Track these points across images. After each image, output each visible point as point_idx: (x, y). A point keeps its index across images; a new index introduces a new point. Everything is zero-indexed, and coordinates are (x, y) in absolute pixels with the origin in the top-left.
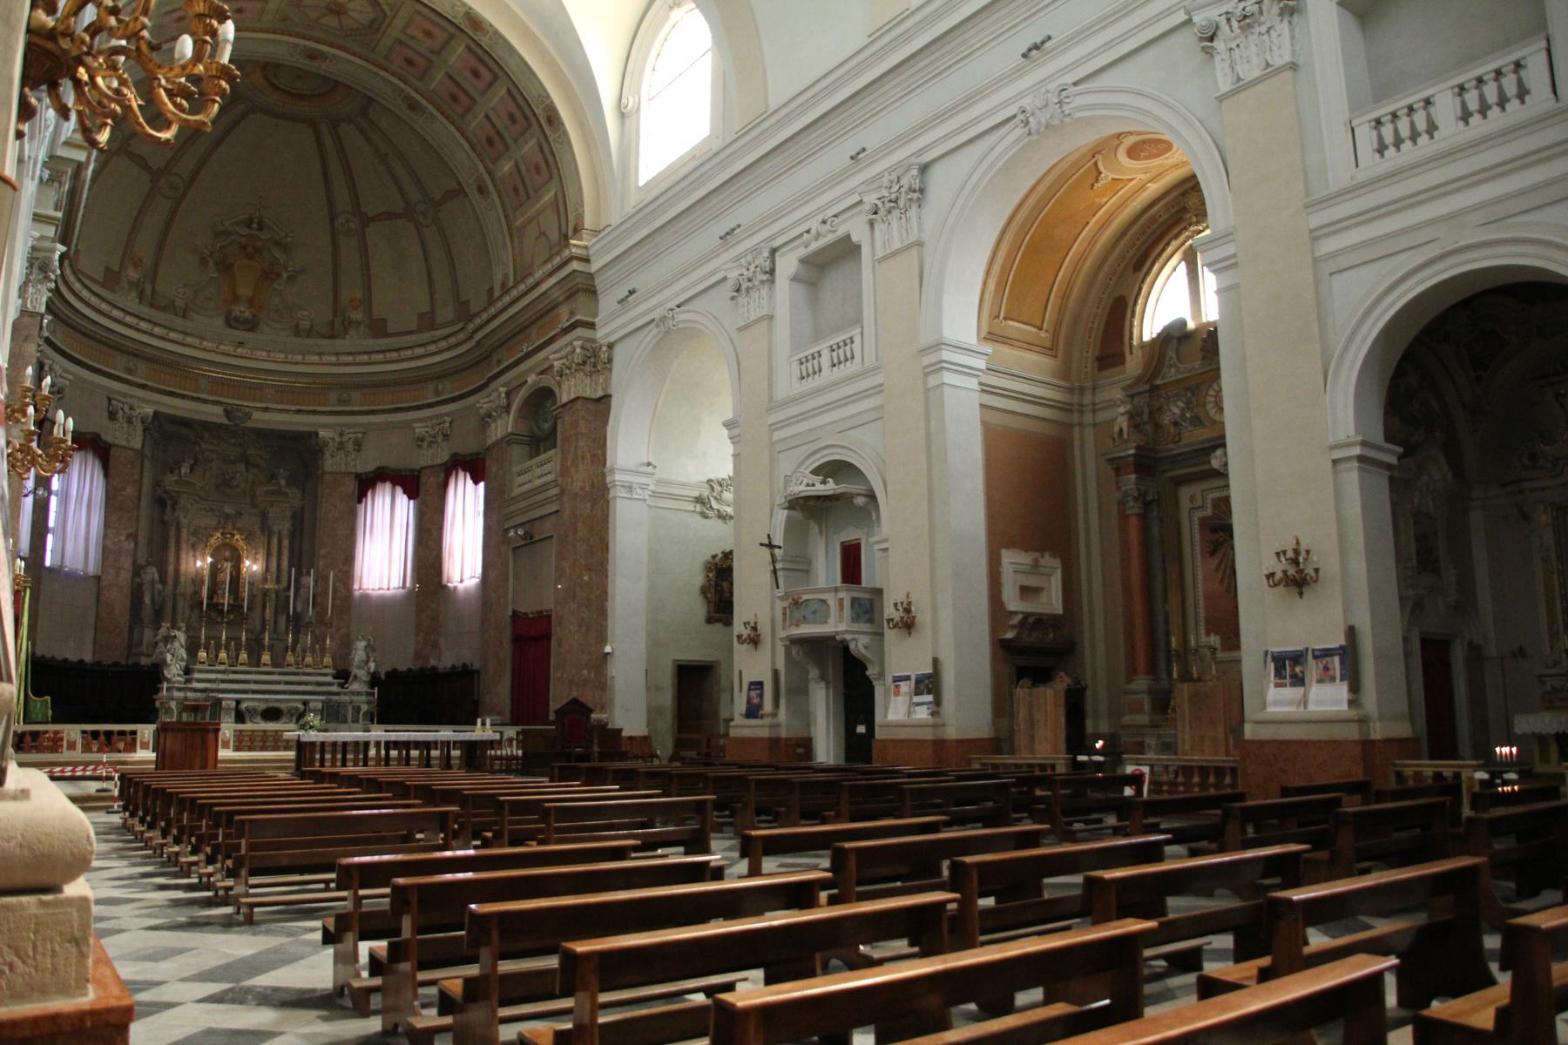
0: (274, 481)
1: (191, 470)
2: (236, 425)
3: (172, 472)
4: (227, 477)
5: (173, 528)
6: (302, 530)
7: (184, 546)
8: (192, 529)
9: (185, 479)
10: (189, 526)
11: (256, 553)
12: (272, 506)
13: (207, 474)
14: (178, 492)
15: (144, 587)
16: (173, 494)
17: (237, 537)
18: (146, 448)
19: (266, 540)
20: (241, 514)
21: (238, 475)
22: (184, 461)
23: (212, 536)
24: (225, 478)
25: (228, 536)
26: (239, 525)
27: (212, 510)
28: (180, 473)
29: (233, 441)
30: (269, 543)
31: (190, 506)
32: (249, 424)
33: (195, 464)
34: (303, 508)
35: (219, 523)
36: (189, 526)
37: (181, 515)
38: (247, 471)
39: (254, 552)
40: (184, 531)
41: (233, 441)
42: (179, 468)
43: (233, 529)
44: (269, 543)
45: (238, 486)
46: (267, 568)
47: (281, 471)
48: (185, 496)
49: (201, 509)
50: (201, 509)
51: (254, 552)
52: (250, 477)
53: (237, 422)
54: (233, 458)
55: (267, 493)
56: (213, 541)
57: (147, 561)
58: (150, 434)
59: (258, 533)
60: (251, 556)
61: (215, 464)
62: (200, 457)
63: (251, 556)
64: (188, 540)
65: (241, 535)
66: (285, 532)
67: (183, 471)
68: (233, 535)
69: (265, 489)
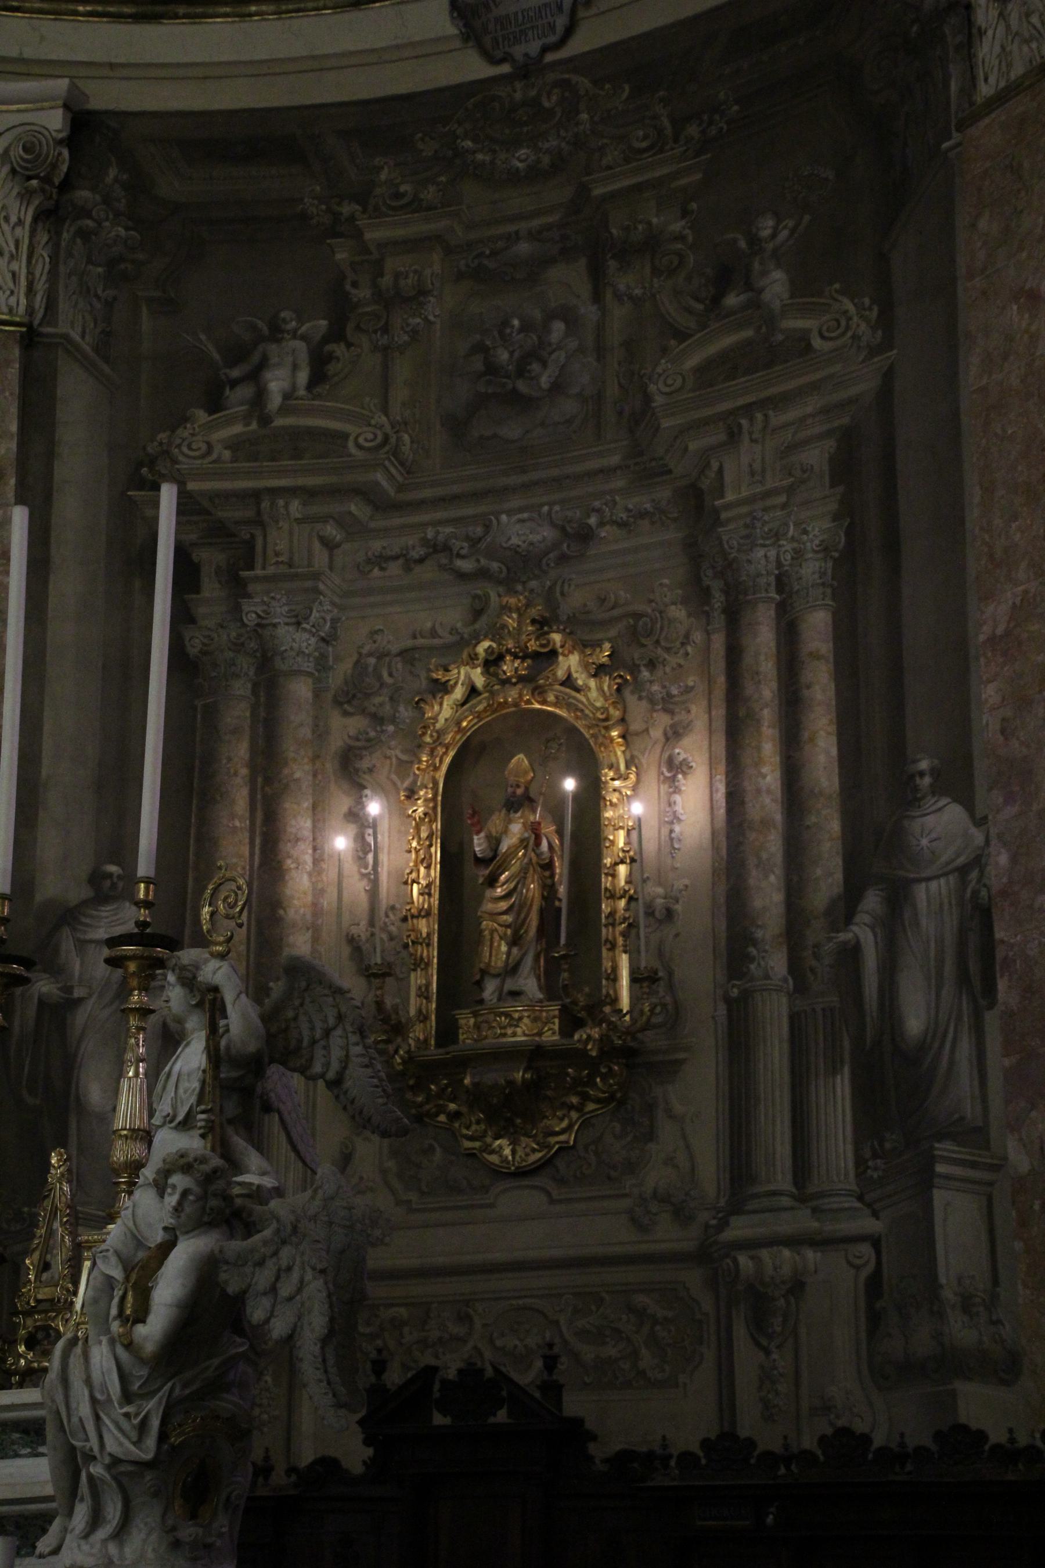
0: (732, 300)
1: (317, 377)
2: (526, 71)
3: (214, 404)
4: (504, 356)
5: (241, 688)
6: (892, 546)
7: (299, 770)
8: (342, 671)
9: (279, 422)
10: (322, 664)
11: (674, 734)
12: (734, 436)
13: (403, 370)
14: (256, 495)
15: (80, 1017)
16: (229, 514)
17: (571, 663)
18: (63, 306)
19: (719, 642)
20: (585, 536)
21: (558, 328)
22: (276, 333)
23: (443, 688)
24: (492, 369)
25: (508, 667)
26: (576, 599)
27: (437, 548)
28: (260, 396)
29: (521, 158)
30: (734, 654)
31: (320, 557)
32: (579, 45)
33: (336, 334)
34: (885, 394)
35: (477, 613)
36: (322, 664)
37: (280, 611)
38: (597, 297)
39: (657, 733)
40: (301, 690)
41: (521, 158)
42: (255, 375)
43: (542, 625)
44: (734, 654)
45: (557, 388)
46: (735, 799)
47: (766, 226)
48: (295, 507)
49: (381, 560)
50: (381, 560)
51: (663, 720)
52: (619, 313)
53: (518, 51)
54: (524, 248)
55: (700, 370)
56: (444, 710)
57: (96, 878)
58: (84, 234)
59: (678, 612)
60: (651, 760)
61: (433, 309)
62: (363, 293)
63: (651, 760)
64: (321, 734)
65: (585, 645)
66: (810, 570)
67: (276, 383)
68: (553, 654)
69: (693, 361)
